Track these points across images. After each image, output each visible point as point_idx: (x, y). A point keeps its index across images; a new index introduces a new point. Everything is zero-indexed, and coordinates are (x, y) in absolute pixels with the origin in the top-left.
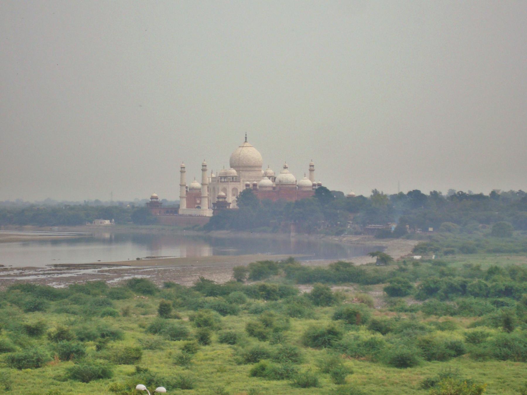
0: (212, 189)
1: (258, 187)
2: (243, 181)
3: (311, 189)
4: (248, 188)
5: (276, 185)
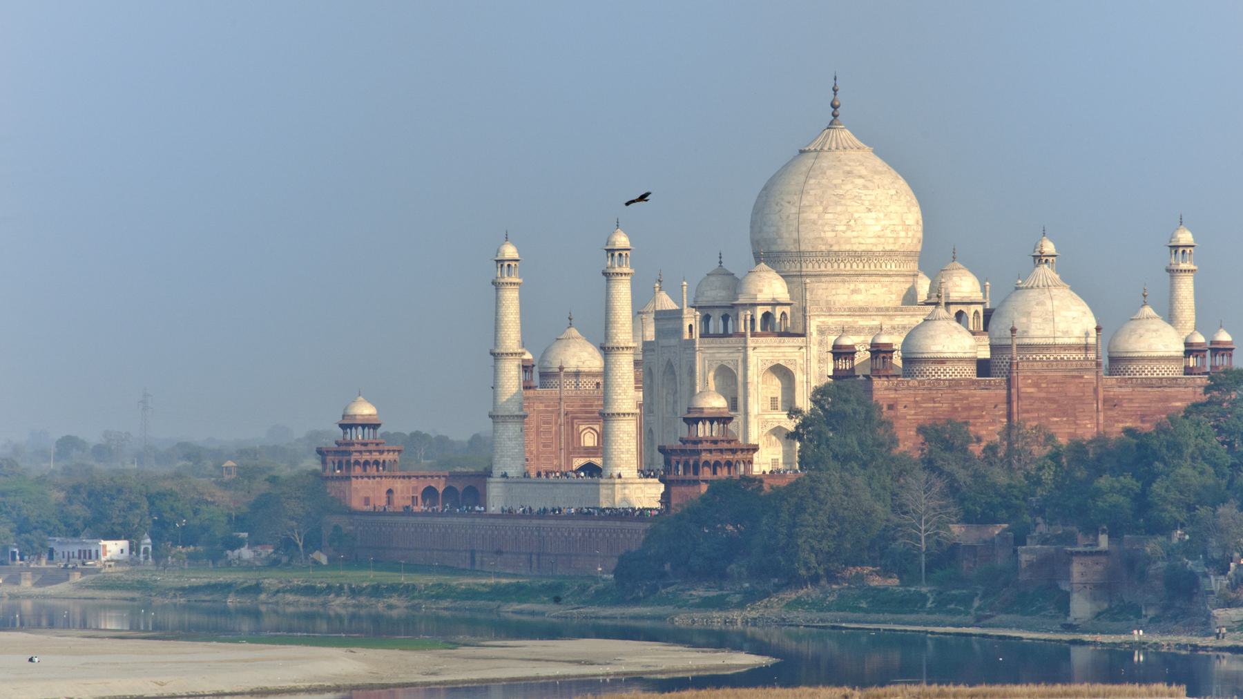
0: (664, 367)
1: (897, 360)
2: (821, 332)
3: (1175, 371)
4: (844, 365)
5: (993, 348)
